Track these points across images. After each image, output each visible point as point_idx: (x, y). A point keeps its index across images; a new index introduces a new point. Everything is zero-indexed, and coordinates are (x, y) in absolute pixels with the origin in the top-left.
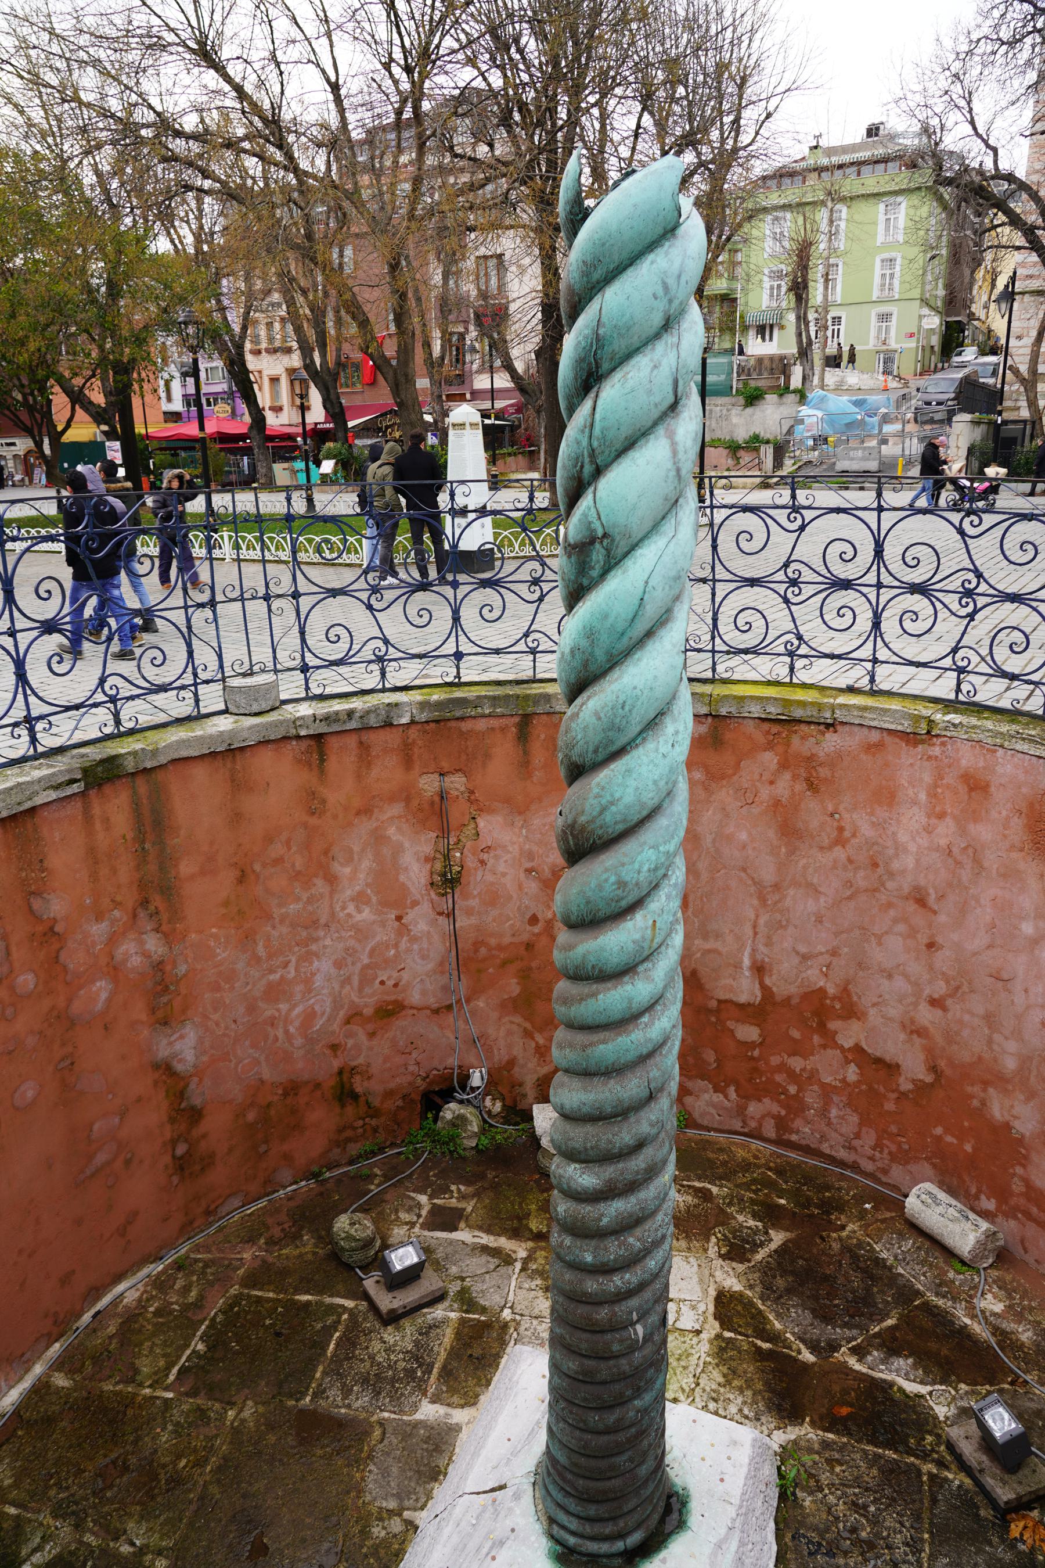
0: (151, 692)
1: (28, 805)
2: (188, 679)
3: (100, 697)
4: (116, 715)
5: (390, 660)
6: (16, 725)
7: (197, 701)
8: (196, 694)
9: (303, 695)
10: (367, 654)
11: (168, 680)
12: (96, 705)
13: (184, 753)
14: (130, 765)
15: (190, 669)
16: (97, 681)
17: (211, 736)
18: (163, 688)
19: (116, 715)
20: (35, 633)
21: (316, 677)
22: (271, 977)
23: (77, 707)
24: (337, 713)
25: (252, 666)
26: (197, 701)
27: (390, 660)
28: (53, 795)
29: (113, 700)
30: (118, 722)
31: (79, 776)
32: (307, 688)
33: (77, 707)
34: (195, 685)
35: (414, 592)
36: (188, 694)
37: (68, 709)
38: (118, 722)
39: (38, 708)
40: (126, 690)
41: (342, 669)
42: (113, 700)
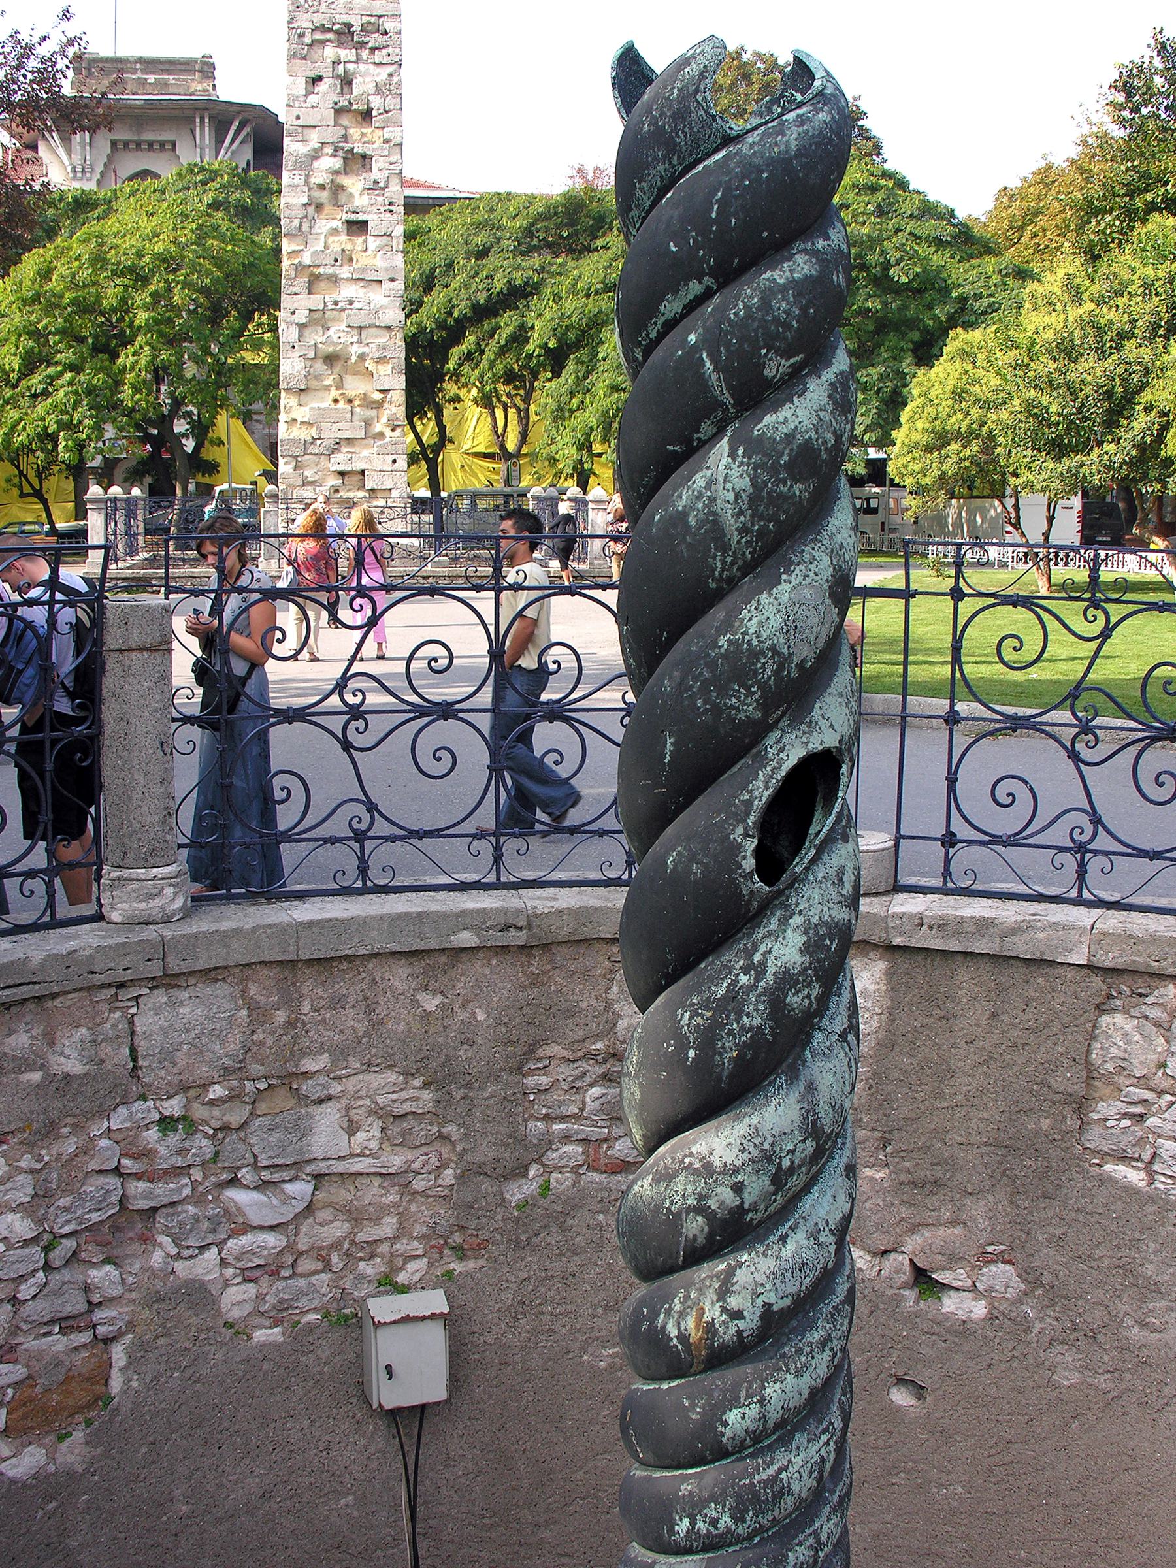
5: (1096, 852)
9: (937, 882)
10: (1058, 835)
21: (963, 857)
24: (961, 921)
27: (1096, 852)
32: (947, 874)
35: (1154, 740)
41: (1010, 852)
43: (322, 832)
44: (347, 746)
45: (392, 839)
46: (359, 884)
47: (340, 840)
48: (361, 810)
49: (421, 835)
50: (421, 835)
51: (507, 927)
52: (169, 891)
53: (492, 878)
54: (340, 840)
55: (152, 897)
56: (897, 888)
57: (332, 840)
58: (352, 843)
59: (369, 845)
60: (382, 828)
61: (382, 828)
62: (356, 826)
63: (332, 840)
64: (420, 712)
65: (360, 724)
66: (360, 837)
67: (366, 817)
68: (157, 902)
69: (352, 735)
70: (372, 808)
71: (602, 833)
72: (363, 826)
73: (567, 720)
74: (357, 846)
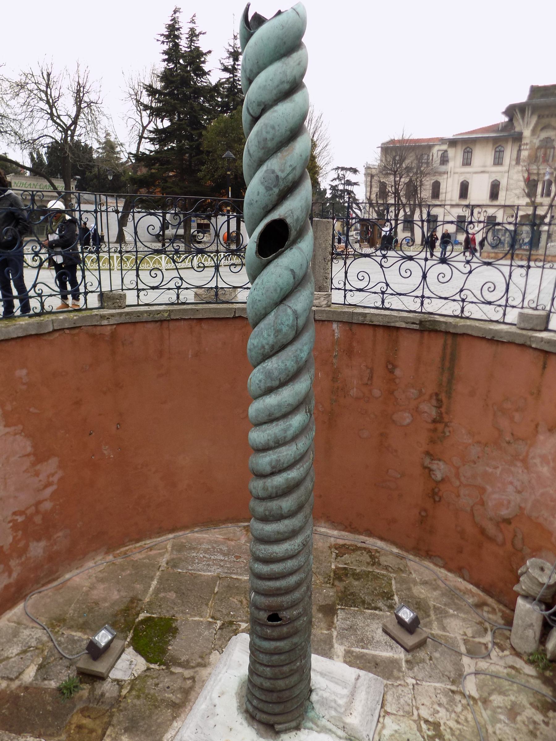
0: (483, 303)
1: (392, 324)
2: (503, 302)
3: (457, 297)
4: (463, 308)
6: (417, 297)
7: (504, 314)
8: (505, 311)
11: (492, 300)
12: (454, 300)
13: (469, 332)
14: (443, 328)
15: (505, 298)
16: (459, 290)
17: (485, 329)
18: (490, 303)
19: (463, 308)
20: (436, 262)
22: (487, 469)
23: (446, 298)
25: (537, 306)
26: (504, 314)
28: (403, 325)
29: (463, 301)
30: (462, 311)
31: (418, 323)
33: (446, 298)
34: (506, 306)
36: (501, 310)
37: (441, 298)
38: (462, 311)
39: (427, 293)
40: (471, 298)
42: (463, 301)
43: (373, 290)
44: (382, 266)
45: (392, 294)
46: (381, 306)
47: (377, 293)
48: (384, 285)
49: (400, 294)
50: (400, 294)
51: (413, 323)
52: (322, 299)
53: (419, 310)
54: (377, 293)
55: (317, 299)
56: (546, 329)
57: (375, 293)
58: (380, 294)
59: (385, 296)
60: (389, 291)
61: (389, 291)
62: (382, 289)
63: (375, 293)
64: (403, 258)
65: (386, 260)
66: (383, 293)
67: (385, 287)
68: (317, 301)
69: (383, 263)
70: (387, 285)
71: (454, 300)
72: (384, 290)
73: (448, 264)
74: (382, 295)
